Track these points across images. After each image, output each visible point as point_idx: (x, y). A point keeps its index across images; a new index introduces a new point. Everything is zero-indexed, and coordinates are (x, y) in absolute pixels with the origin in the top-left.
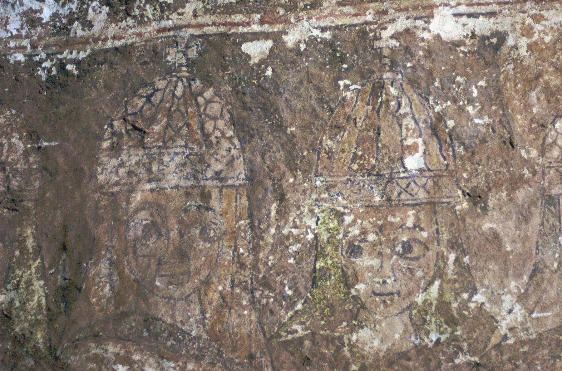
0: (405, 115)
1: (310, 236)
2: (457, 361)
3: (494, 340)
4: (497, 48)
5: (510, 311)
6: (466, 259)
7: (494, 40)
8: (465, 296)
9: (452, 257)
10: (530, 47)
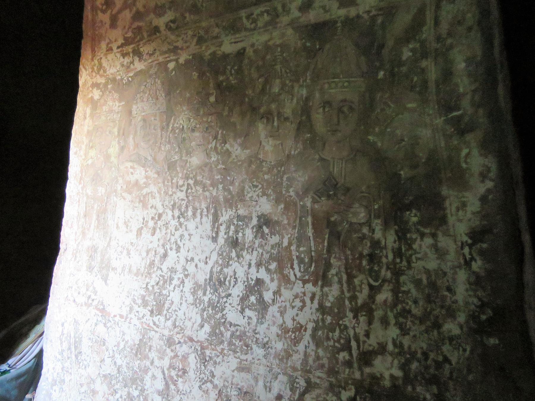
1: (181, 127)
2: (218, 167)
4: (243, 54)
7: (242, 51)
8: (223, 145)
9: (220, 132)
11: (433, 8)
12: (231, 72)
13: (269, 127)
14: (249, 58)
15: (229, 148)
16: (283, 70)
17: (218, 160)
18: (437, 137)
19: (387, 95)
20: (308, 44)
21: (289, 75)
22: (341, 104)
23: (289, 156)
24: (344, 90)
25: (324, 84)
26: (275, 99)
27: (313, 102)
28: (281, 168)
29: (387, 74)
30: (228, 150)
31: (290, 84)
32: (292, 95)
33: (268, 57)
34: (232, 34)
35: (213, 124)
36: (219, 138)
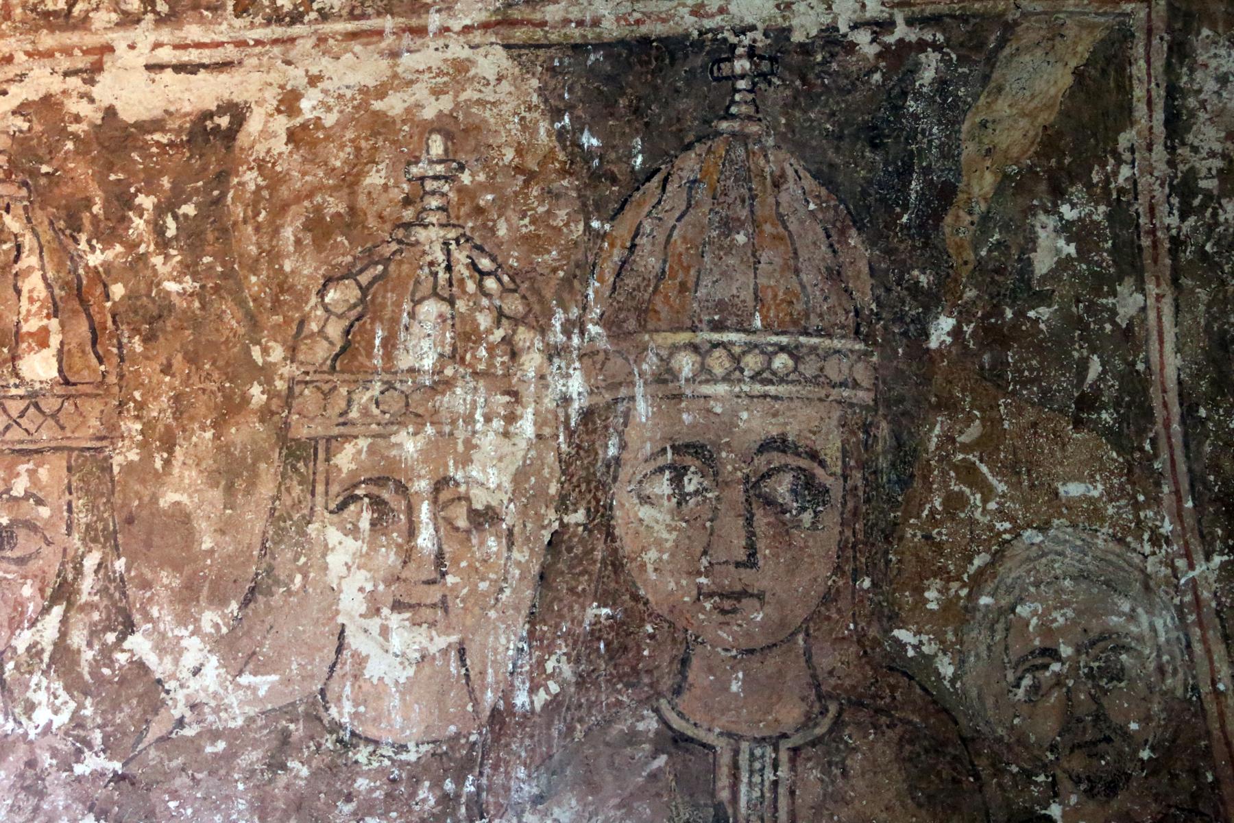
0: (29, 270)
2: (79, 769)
3: (156, 730)
4: (230, 135)
5: (196, 672)
6: (120, 565)
7: (224, 121)
8: (111, 637)
9: (91, 562)
10: (292, 136)
11: (1160, 47)
12: (159, 230)
13: (389, 558)
14: (261, 165)
15: (151, 660)
16: (460, 257)
17: (78, 722)
18: (1198, 648)
19: (974, 431)
20: (590, 141)
21: (491, 283)
22: (761, 462)
23: (499, 719)
24: (772, 389)
25: (675, 349)
26: (416, 403)
27: (623, 446)
28: (460, 781)
29: (968, 329)
30: (140, 667)
31: (498, 334)
32: (515, 394)
33: (375, 178)
34: (161, 21)
35: (44, 512)
36: (84, 598)
